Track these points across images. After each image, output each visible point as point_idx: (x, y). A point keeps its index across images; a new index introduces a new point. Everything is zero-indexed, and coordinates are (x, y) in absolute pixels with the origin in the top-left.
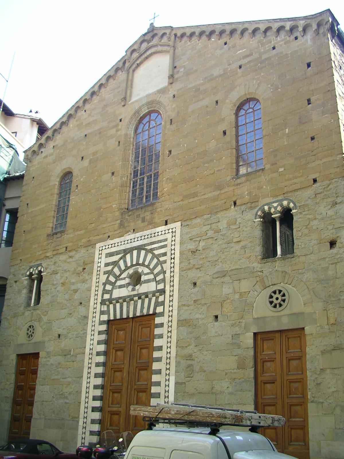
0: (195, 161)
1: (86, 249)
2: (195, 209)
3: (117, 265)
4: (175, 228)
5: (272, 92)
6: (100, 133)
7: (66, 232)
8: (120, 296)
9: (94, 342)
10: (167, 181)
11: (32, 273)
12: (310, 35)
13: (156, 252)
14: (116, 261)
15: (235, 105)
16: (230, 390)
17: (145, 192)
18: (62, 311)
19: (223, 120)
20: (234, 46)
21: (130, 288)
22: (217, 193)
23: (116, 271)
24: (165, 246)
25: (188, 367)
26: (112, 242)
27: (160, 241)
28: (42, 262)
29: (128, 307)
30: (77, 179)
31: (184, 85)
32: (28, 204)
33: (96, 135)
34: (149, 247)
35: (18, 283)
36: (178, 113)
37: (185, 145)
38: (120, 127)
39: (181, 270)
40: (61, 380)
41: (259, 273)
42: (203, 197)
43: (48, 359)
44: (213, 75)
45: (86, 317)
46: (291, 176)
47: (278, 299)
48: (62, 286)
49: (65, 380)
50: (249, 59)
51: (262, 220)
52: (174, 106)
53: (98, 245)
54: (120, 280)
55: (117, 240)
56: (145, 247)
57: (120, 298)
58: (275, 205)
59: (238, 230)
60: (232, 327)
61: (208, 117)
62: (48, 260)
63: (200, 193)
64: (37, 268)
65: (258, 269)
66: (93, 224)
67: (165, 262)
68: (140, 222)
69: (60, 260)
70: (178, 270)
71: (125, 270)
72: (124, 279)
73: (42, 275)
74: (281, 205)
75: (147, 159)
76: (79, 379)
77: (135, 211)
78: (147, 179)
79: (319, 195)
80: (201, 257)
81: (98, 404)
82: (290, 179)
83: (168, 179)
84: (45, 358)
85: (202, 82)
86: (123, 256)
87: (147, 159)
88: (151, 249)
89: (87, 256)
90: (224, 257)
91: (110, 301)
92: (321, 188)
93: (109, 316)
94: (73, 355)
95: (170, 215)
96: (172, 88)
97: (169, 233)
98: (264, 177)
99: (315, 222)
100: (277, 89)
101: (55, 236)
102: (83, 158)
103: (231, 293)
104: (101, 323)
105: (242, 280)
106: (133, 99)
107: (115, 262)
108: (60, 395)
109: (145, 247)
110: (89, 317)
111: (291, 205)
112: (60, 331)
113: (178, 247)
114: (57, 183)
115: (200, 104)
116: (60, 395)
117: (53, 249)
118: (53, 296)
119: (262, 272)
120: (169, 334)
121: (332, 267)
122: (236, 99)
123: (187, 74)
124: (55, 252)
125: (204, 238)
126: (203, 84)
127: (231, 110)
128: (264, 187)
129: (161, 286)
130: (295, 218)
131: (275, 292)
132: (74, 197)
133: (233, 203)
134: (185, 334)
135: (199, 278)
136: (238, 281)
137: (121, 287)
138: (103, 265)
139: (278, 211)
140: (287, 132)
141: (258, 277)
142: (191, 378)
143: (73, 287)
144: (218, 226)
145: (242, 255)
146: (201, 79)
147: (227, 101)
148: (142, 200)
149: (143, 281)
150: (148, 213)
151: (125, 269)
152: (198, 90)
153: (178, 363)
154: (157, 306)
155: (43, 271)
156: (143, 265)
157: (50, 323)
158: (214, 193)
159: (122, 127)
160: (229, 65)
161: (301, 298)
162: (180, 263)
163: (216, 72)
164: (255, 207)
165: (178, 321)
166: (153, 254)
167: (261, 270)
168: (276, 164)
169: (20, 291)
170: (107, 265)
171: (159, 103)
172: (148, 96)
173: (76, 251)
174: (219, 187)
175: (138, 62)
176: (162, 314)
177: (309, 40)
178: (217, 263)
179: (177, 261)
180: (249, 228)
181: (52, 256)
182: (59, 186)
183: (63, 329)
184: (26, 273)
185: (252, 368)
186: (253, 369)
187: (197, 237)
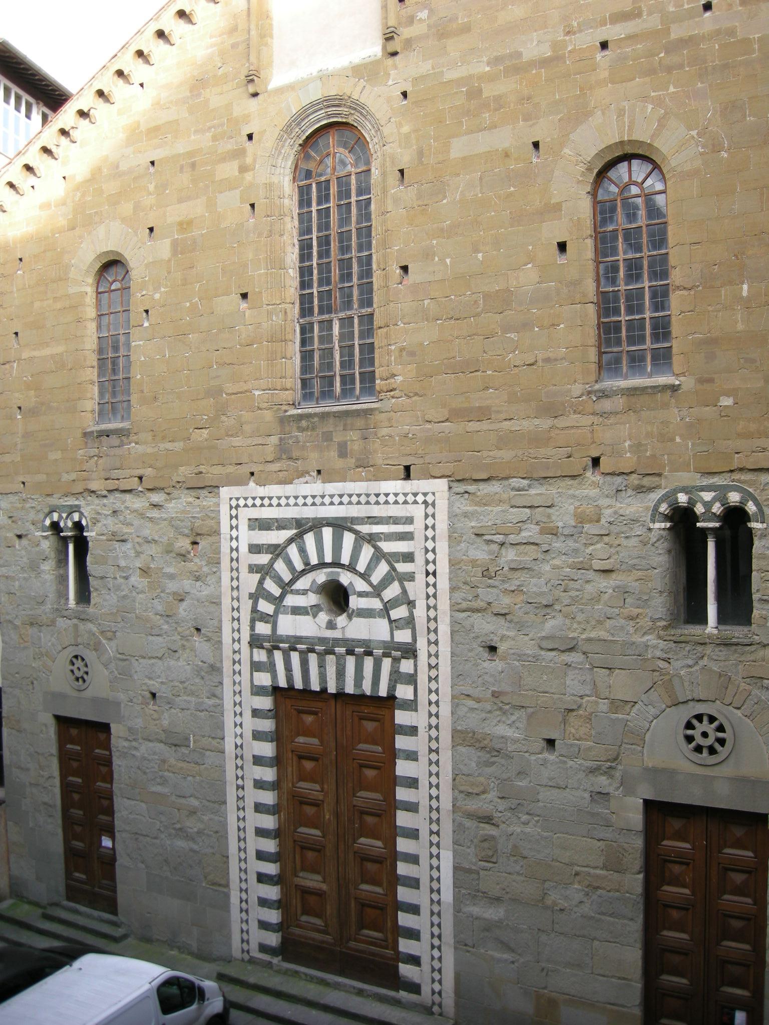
0: (477, 315)
1: (194, 493)
2: (485, 454)
4: (434, 494)
5: (701, 154)
6: (193, 166)
7: (133, 438)
8: (298, 634)
9: (243, 730)
10: (401, 356)
13: (387, 547)
14: (279, 546)
15: (589, 169)
16: (586, 909)
17: (338, 363)
18: (151, 638)
19: (557, 208)
21: (323, 617)
22: (545, 423)
25: (485, 840)
26: (262, 491)
27: (396, 521)
28: (81, 502)
29: (322, 666)
30: (144, 293)
31: (433, 68)
32: (16, 334)
34: (365, 529)
35: (24, 542)
36: (420, 153)
37: (448, 261)
38: (249, 160)
39: (455, 608)
40: (173, 798)
41: (662, 664)
43: (134, 744)
44: (519, 55)
45: (215, 669)
46: (753, 427)
47: (706, 735)
48: (141, 576)
49: (183, 801)
51: (668, 525)
52: (406, 129)
53: (225, 492)
54: (292, 592)
55: (274, 490)
56: (355, 527)
57: (299, 639)
58: (707, 496)
59: (606, 539)
60: (591, 775)
61: (512, 189)
62: (97, 501)
63: (498, 412)
65: (658, 653)
66: (205, 432)
67: (411, 577)
68: (334, 454)
69: (127, 508)
70: (448, 608)
71: (303, 573)
72: (304, 592)
73: (86, 537)
74: (723, 500)
75: (335, 273)
76: (216, 806)
77: (316, 419)
78: (341, 327)
80: (506, 586)
81: (271, 869)
82: (749, 435)
83: (402, 350)
84: (127, 740)
85: (488, 69)
87: (335, 273)
88: (370, 535)
89: (198, 513)
90: (566, 602)
91: (274, 643)
93: (274, 677)
94: (195, 743)
96: (396, 68)
97: (415, 502)
98: (676, 411)
100: (716, 148)
102: (151, 230)
103: (587, 696)
104: (258, 691)
105: (617, 671)
106: (277, 79)
108: (174, 829)
109: (355, 527)
110: (225, 670)
111: (751, 508)
112: (154, 685)
113: (443, 548)
115: (485, 142)
116: (174, 829)
117: (103, 474)
118: (125, 597)
119: (667, 660)
122: (594, 152)
123: (443, 31)
124: (111, 484)
125: (512, 538)
126: (491, 78)
127: (579, 182)
128: (678, 440)
129: (403, 636)
130: (756, 543)
131: (699, 717)
132: (141, 343)
133: (590, 463)
134: (474, 765)
135: (503, 638)
136: (607, 671)
137: (297, 611)
138: (244, 549)
139: (715, 514)
140: (745, 293)
141: (656, 674)
142: (491, 865)
143: (172, 586)
144: (549, 516)
145: (617, 607)
146: (485, 59)
147: (566, 151)
148: (331, 384)
149: (353, 611)
150: (353, 437)
152: (474, 93)
153: (458, 829)
154: (396, 682)
155: (87, 525)
156: (351, 568)
158: (537, 422)
159: (255, 161)
160: (569, 32)
161: (765, 748)
162: (453, 589)
163: (533, 47)
164: (651, 489)
165: (455, 732)
166: (376, 548)
167: (665, 656)
168: (711, 381)
169: (34, 566)
170: (255, 549)
171: (357, 107)
172: (324, 77)
173: (169, 494)
174: (552, 410)
176: (411, 705)
178: (548, 610)
179: (443, 583)
180: (633, 542)
182: (95, 294)
183: (162, 683)
184: (44, 521)
185: (639, 873)
186: (641, 876)
187: (493, 532)
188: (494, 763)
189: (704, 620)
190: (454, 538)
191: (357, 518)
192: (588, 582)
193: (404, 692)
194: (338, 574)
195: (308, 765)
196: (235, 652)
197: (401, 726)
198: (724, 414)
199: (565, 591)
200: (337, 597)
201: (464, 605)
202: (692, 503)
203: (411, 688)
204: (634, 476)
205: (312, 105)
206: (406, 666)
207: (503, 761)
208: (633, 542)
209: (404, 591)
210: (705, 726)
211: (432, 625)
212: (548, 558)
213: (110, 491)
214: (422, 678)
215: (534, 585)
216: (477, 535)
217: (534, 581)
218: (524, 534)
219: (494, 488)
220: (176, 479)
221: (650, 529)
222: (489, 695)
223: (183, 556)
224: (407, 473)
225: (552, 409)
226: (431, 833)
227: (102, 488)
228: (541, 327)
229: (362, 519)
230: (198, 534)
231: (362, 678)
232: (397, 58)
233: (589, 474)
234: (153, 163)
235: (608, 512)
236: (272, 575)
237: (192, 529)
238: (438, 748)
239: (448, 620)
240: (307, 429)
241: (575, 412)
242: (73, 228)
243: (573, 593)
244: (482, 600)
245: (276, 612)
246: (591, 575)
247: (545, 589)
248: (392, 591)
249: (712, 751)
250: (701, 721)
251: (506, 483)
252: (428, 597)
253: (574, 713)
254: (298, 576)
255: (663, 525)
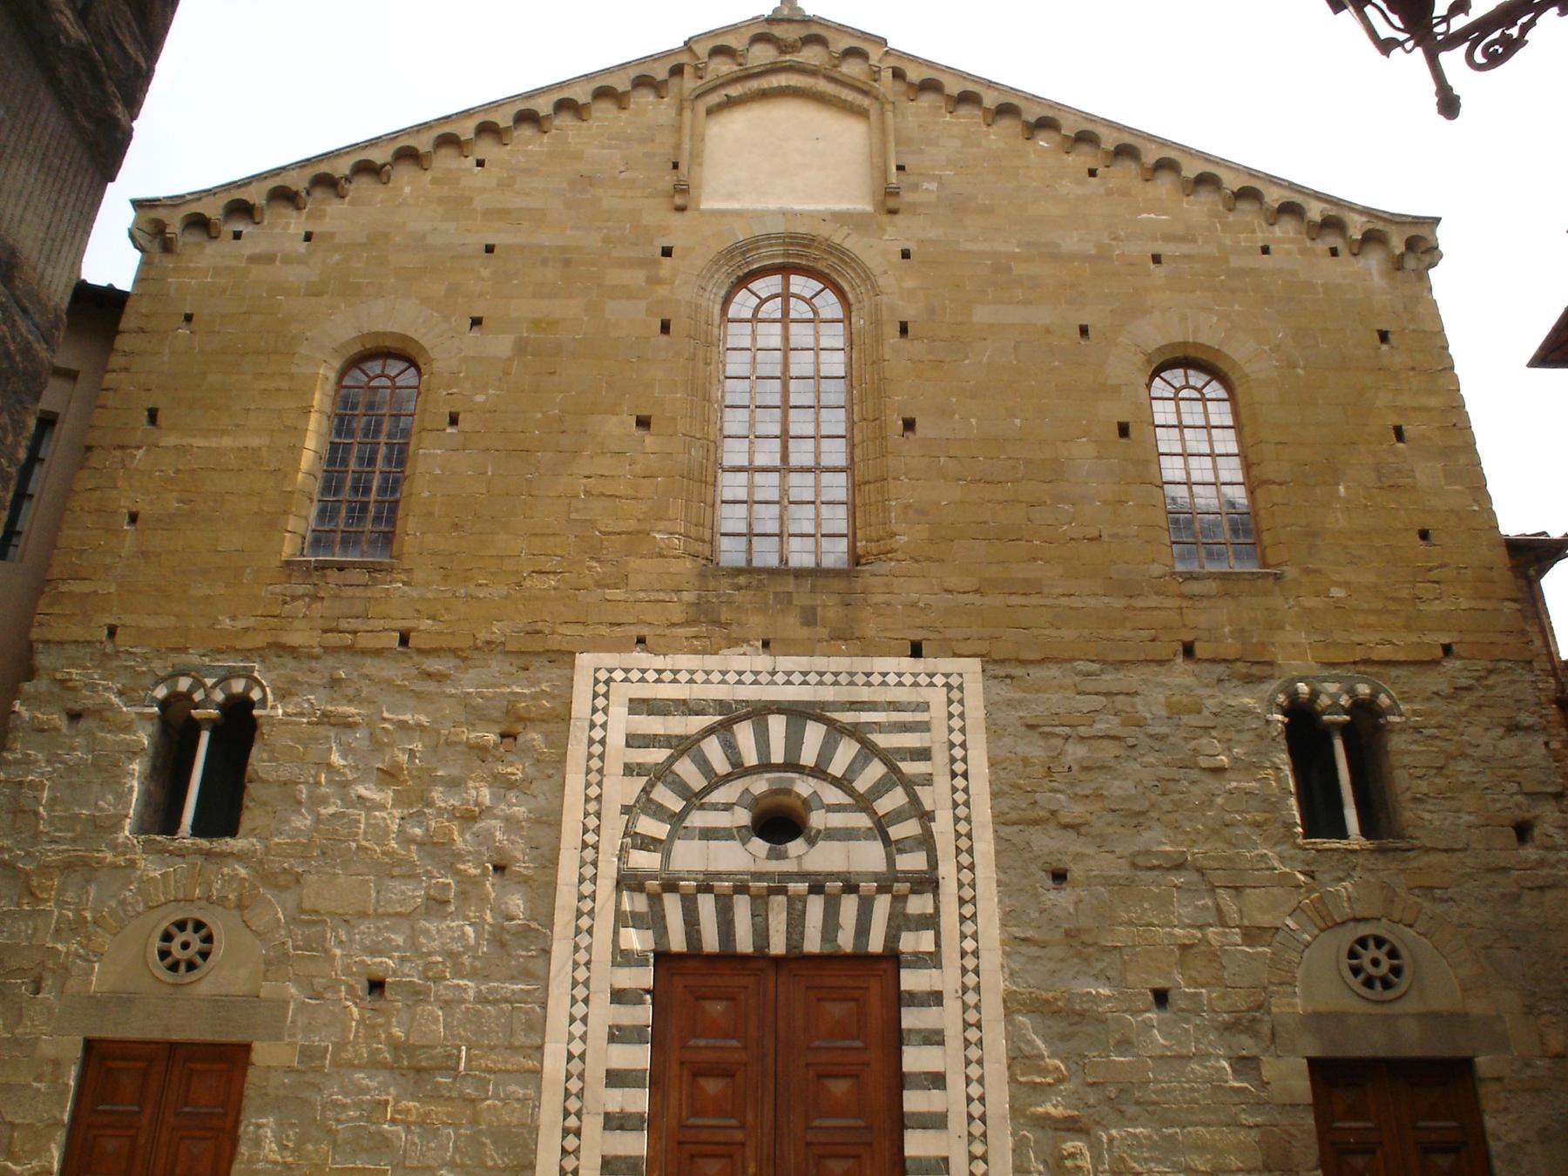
1: (519, 662)
3: (692, 752)
4: (961, 675)
8: (712, 868)
11: (188, 696)
12: (1373, 262)
13: (883, 740)
14: (687, 737)
15: (1149, 361)
19: (1116, 389)
20: (1125, 192)
22: (1120, 603)
23: (686, 769)
24: (924, 727)
26: (659, 662)
33: (545, 262)
36: (931, 311)
37: (973, 421)
39: (1000, 820)
42: (1064, 601)
47: (1376, 965)
50: (1185, 249)
54: (702, 807)
55: (684, 661)
58: (1332, 687)
62: (291, 663)
64: (225, 679)
67: (928, 780)
69: (367, 677)
71: (727, 779)
72: (728, 807)
74: (1351, 692)
79: (1465, 694)
80: (1078, 790)
83: (907, 507)
86: (720, 723)
90: (1166, 807)
92: (1466, 673)
95: (929, 628)
97: (931, 684)
99: (1465, 766)
100: (1293, 366)
101: (333, 575)
107: (681, 738)
111: (1384, 700)
114: (333, 376)
117: (321, 623)
120: (973, 1035)
121: (1527, 897)
122: (1155, 346)
124: (333, 639)
125: (1082, 730)
129: (913, 862)
131: (1362, 942)
135: (1079, 857)
137: (708, 834)
138: (616, 738)
144: (1133, 705)
149: (819, 832)
151: (729, 774)
156: (819, 772)
157: (314, 923)
158: (1106, 600)
163: (1071, 242)
164: (1262, 679)
173: (465, 659)
175: (735, 91)
177: (1375, 273)
181: (318, 650)
188: (1072, 1036)
189: (1342, 833)
190: (994, 730)
191: (833, 703)
192: (1193, 782)
193: (910, 942)
194: (792, 781)
195: (712, 1086)
196: (581, 898)
197: (911, 994)
198: (1339, 606)
199: (1164, 794)
200: (778, 823)
201: (1014, 816)
202: (1315, 694)
203: (930, 934)
204: (1239, 664)
205: (769, 237)
206: (918, 905)
207: (1090, 1029)
208: (1248, 736)
209: (914, 800)
210: (1372, 952)
211: (964, 843)
212: (1134, 754)
213: (329, 650)
214: (949, 920)
215: (1117, 788)
216: (1030, 727)
217: (1117, 783)
218: (1098, 726)
219: (1053, 671)
220: (483, 636)
221: (1268, 722)
222: (1058, 935)
223: (481, 750)
224: (916, 651)
225: (1128, 589)
226: (972, 1158)
227: (315, 644)
228: (1105, 502)
229: (844, 703)
230: (520, 719)
231: (837, 927)
232: (896, 218)
233: (1179, 660)
234: (489, 249)
235: (1209, 702)
236: (670, 779)
237: (508, 712)
238: (979, 1020)
239: (989, 835)
240: (748, 587)
241: (1157, 593)
242: (318, 294)
243: (1176, 797)
244: (1043, 808)
245: (672, 835)
246: (1194, 774)
247: (1133, 792)
248: (895, 799)
249: (1387, 985)
250: (1365, 947)
251: (1068, 666)
252: (955, 805)
253: (1195, 950)
254: (716, 781)
255: (1280, 717)
